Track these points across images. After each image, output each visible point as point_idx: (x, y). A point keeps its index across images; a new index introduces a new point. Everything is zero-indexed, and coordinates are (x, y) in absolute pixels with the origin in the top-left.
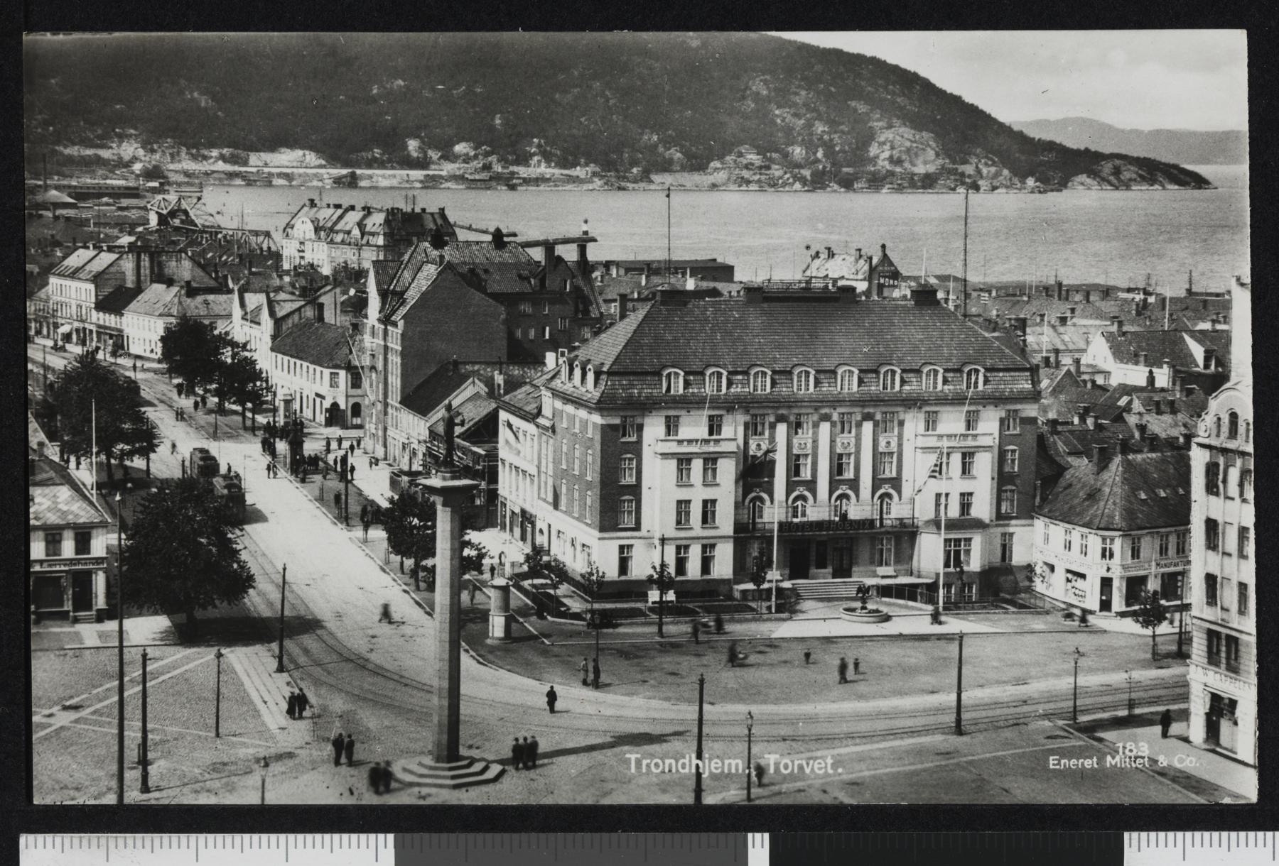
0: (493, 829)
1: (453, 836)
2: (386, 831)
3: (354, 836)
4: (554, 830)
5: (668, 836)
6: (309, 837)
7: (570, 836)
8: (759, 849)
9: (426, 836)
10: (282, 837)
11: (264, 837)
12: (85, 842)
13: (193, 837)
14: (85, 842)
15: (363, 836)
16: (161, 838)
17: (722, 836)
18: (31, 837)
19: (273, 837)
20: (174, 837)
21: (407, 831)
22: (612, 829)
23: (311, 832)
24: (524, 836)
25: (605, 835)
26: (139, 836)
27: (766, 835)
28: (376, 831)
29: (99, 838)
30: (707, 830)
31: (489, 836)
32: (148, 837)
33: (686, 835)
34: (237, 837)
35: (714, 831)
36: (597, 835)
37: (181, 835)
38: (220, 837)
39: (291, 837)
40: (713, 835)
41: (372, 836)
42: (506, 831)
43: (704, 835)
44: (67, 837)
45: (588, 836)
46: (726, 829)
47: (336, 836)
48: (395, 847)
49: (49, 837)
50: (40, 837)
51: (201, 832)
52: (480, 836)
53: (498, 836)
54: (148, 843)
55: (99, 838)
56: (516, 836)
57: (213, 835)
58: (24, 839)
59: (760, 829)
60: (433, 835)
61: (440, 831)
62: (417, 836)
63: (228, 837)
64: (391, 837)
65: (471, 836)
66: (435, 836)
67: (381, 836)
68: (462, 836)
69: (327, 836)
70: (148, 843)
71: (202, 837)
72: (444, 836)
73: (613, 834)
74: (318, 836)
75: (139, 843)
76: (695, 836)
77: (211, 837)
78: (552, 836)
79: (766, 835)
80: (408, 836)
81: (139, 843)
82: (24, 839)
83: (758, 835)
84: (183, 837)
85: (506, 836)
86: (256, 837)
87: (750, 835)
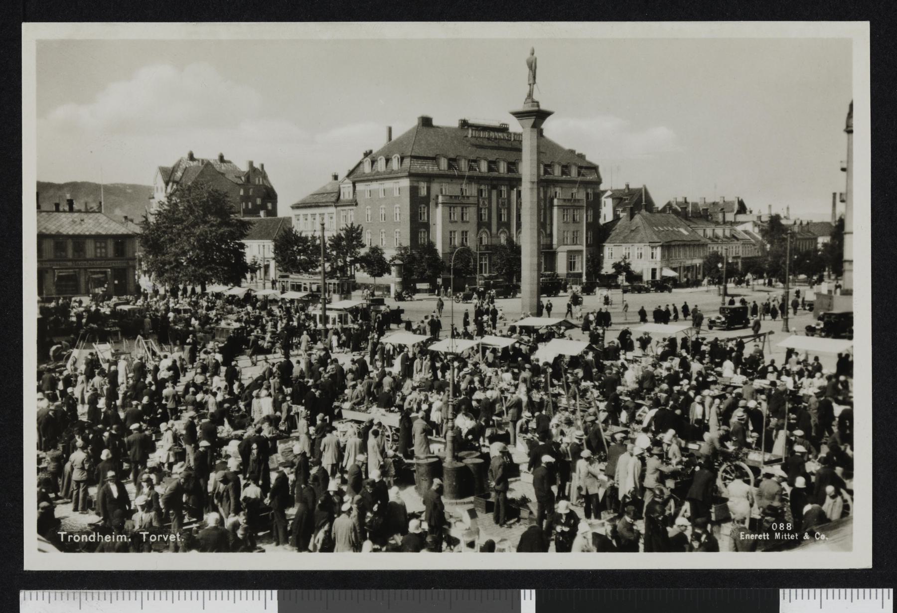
0: (345, 587)
1: (318, 591)
2: (271, 587)
3: (250, 592)
4: (388, 588)
5: (466, 591)
6: (219, 592)
7: (398, 591)
8: (528, 601)
9: (299, 591)
10: (201, 592)
11: (188, 592)
12: (65, 596)
13: (139, 592)
14: (65, 596)
15: (256, 592)
16: (117, 593)
17: (503, 591)
18: (28, 592)
19: (194, 592)
20: (126, 592)
21: (286, 588)
22: (428, 587)
23: (220, 589)
24: (367, 591)
25: (423, 591)
26: (102, 591)
27: (534, 591)
28: (265, 588)
29: (74, 593)
30: (493, 587)
31: (343, 591)
32: (108, 592)
33: (478, 591)
34: (170, 592)
35: (498, 588)
36: (417, 591)
37: (131, 591)
38: (157, 592)
39: (207, 592)
40: (497, 591)
41: (262, 592)
42: (354, 588)
43: (491, 591)
44: (52, 592)
45: (410, 591)
46: (506, 587)
47: (238, 592)
48: (278, 599)
49: (40, 592)
50: (34, 592)
51: (145, 589)
52: (337, 592)
53: (349, 592)
54: (108, 597)
55: (74, 593)
56: (361, 592)
57: (153, 591)
58: (22, 594)
59: (530, 587)
60: (304, 591)
61: (309, 588)
62: (293, 591)
63: (163, 592)
64: (275, 592)
65: (330, 592)
66: (305, 592)
67: (268, 592)
68: (324, 592)
69: (231, 592)
70: (108, 597)
71: (145, 592)
72: (312, 592)
73: (428, 591)
74: (225, 592)
75: (102, 596)
76: (484, 591)
77: (151, 592)
78: (386, 592)
79: (534, 591)
80: (287, 592)
81: (102, 596)
82: (24, 594)
83: (528, 591)
84: (132, 592)
85: (355, 592)
86: (182, 592)
87: (522, 591)
